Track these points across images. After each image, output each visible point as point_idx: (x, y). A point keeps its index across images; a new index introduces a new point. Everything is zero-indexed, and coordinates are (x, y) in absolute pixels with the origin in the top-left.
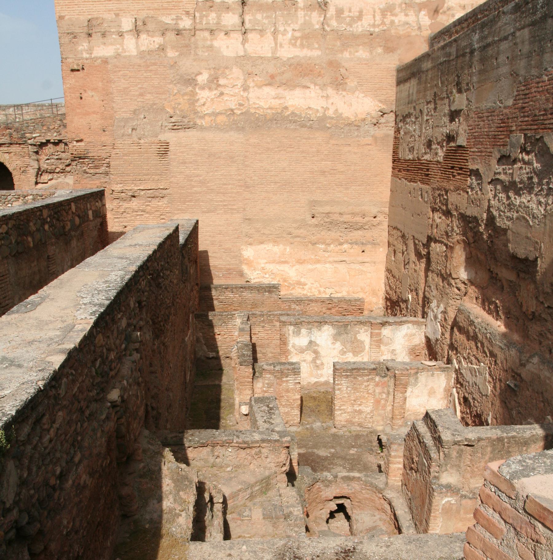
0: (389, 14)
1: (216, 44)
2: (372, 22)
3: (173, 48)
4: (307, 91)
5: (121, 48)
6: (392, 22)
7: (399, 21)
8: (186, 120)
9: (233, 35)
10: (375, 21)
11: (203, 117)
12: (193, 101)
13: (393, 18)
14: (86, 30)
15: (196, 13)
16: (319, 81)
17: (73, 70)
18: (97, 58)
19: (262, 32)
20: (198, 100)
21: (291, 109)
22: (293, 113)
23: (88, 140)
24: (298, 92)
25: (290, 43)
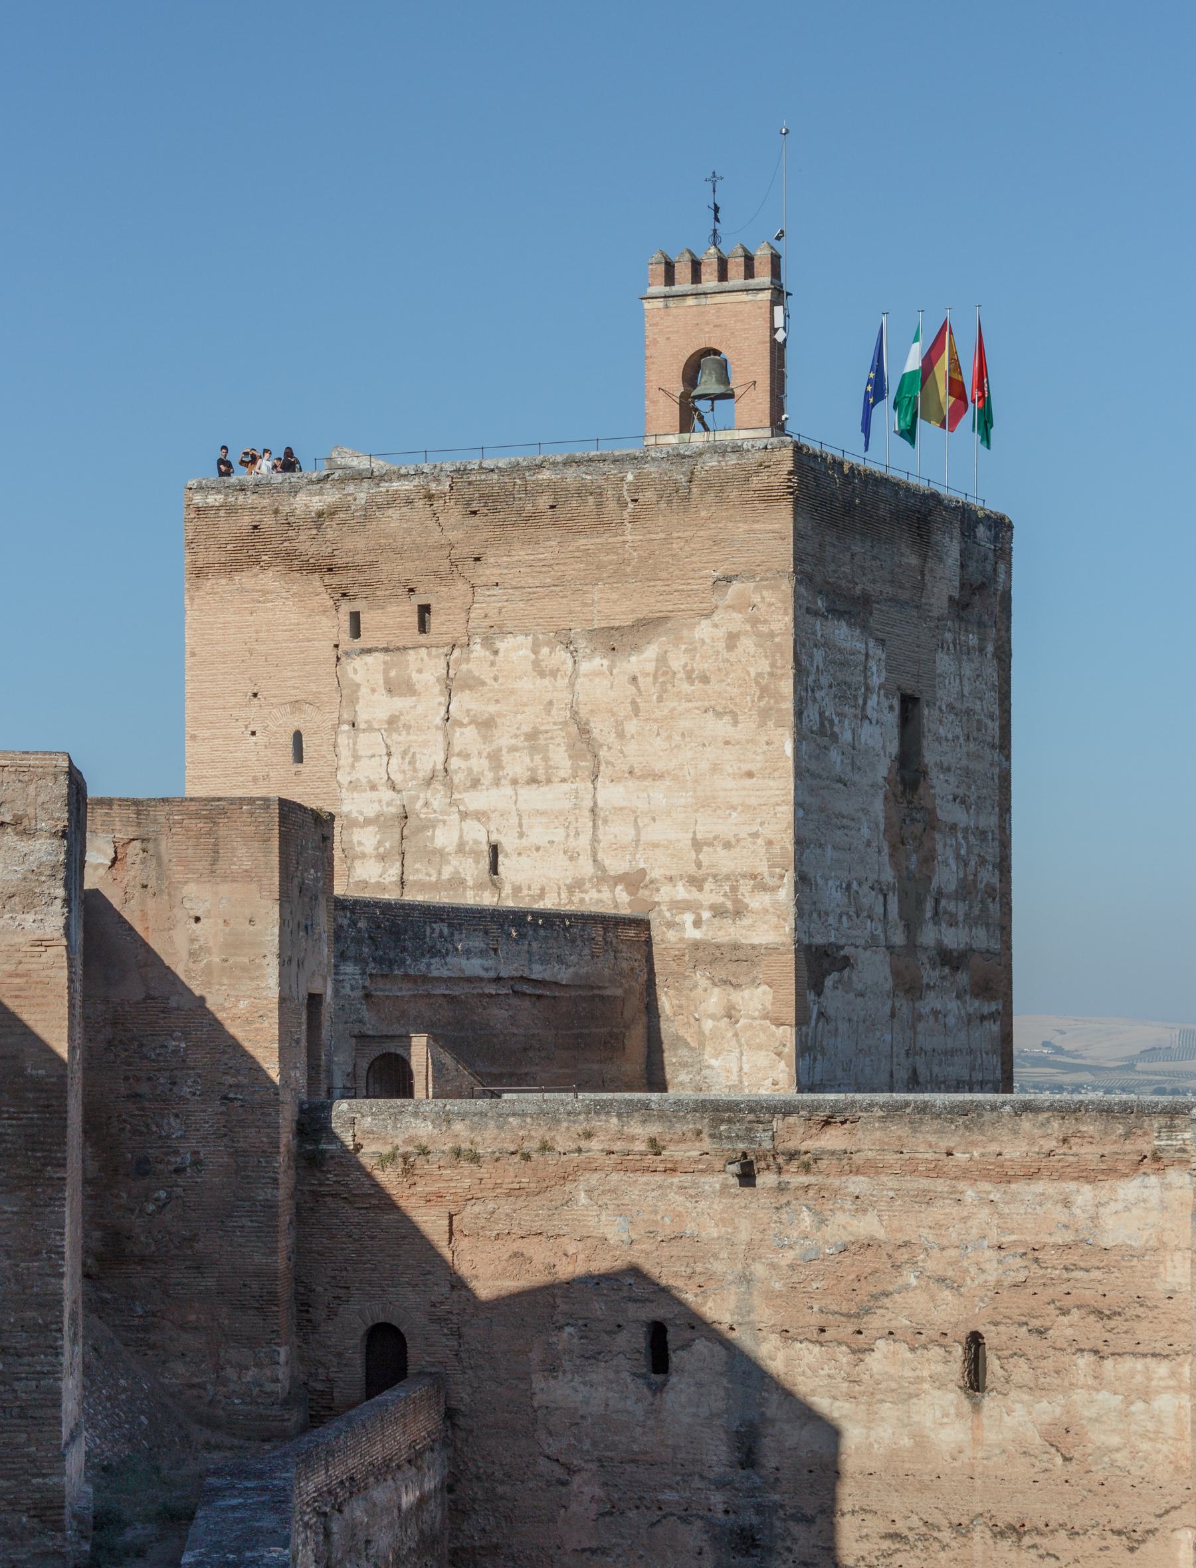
7: (591, 899)
10: (560, 899)
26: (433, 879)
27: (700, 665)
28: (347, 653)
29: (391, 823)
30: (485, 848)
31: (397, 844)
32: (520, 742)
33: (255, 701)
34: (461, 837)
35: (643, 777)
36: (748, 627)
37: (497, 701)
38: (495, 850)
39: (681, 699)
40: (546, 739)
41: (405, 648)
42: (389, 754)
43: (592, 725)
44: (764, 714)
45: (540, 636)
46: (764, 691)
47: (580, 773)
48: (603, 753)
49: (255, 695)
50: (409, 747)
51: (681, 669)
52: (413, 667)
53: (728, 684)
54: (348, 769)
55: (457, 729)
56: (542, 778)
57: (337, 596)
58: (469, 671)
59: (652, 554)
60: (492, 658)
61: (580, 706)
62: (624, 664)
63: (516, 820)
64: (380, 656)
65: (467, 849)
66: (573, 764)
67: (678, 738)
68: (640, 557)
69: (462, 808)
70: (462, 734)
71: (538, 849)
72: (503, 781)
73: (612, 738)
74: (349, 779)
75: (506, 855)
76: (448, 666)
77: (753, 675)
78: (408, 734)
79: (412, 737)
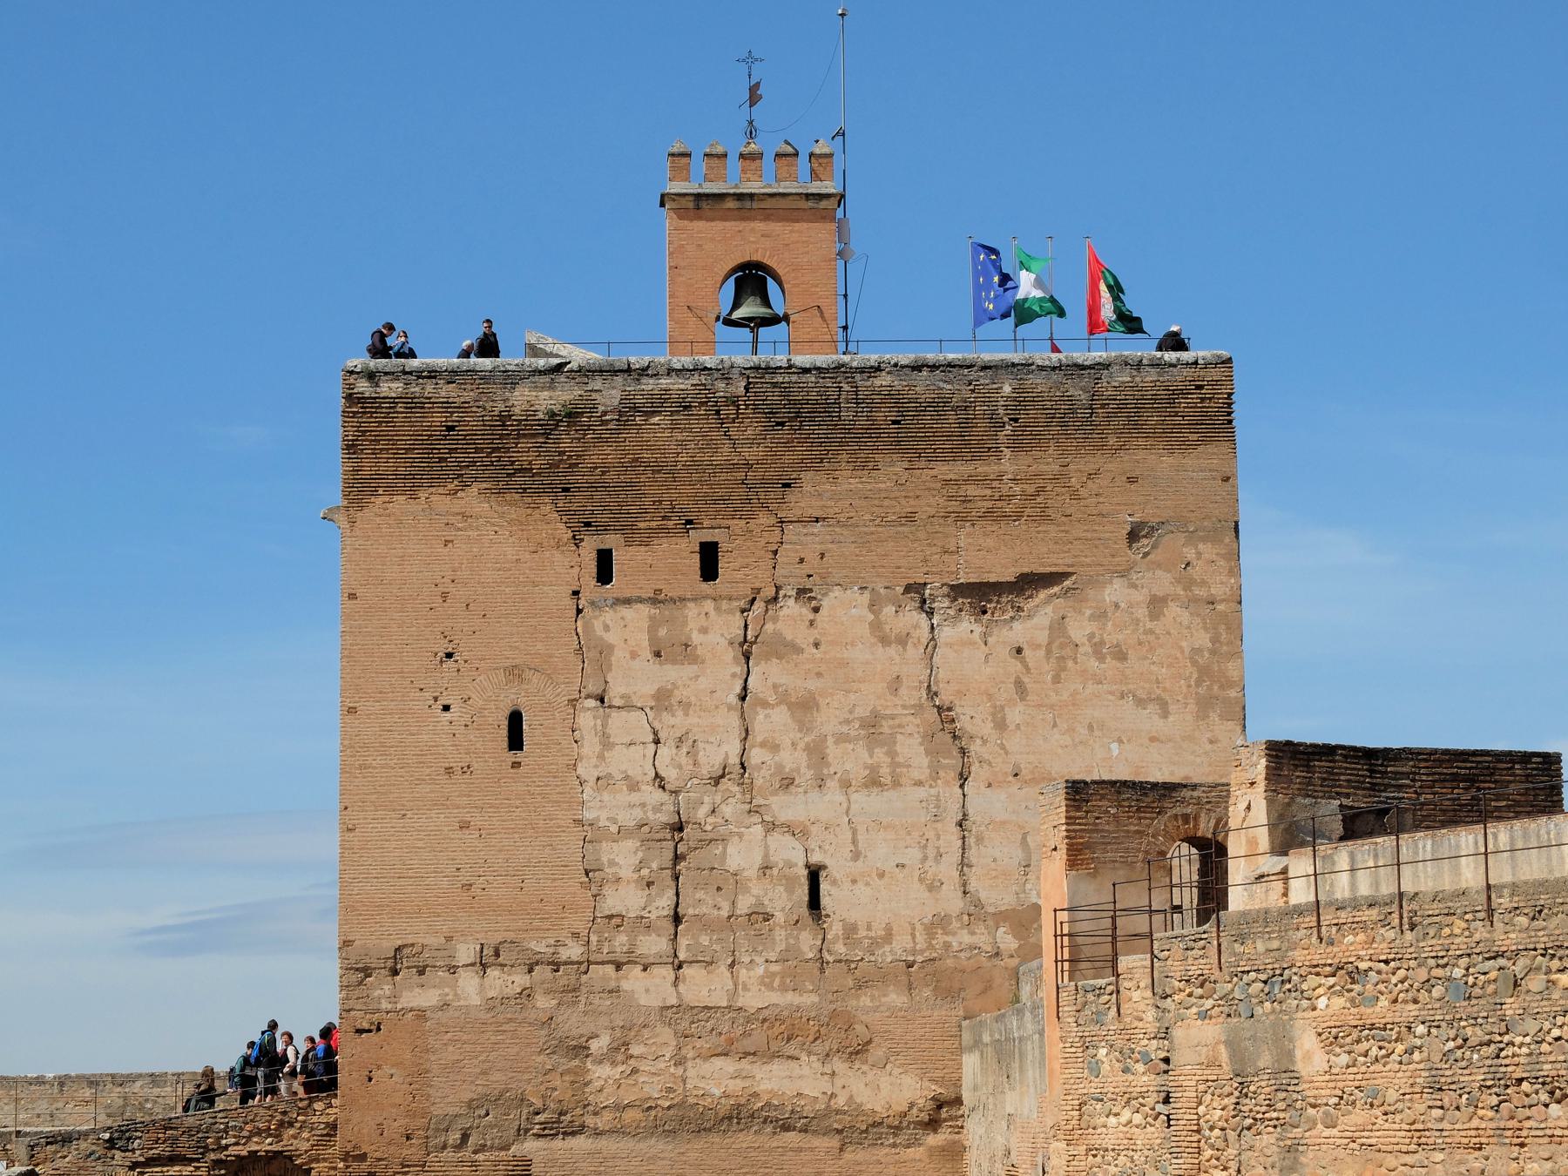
0: (940, 931)
1: (625, 985)
3: (548, 992)
5: (451, 993)
6: (947, 946)
9: (656, 970)
12: (580, 1081)
13: (949, 938)
14: (390, 963)
15: (591, 935)
18: (404, 1011)
21: (765, 1098)
22: (768, 1104)
23: (378, 1155)
24: (778, 1067)
25: (762, 983)
26: (725, 913)
27: (1112, 636)
28: (592, 603)
29: (658, 836)
30: (805, 872)
31: (669, 864)
32: (853, 730)
33: (450, 663)
34: (766, 856)
35: (1034, 781)
37: (819, 675)
38: (814, 876)
40: (891, 727)
41: (682, 600)
42: (657, 742)
43: (958, 709)
44: (1205, 705)
45: (882, 591)
46: (1204, 672)
47: (942, 774)
48: (975, 748)
49: (449, 655)
51: (1085, 640)
52: (693, 626)
53: (1154, 663)
56: (887, 780)
58: (778, 635)
59: (1040, 490)
60: (811, 616)
61: (941, 686)
63: (849, 835)
64: (645, 610)
66: (931, 761)
69: (767, 818)
70: (767, 716)
71: (881, 875)
73: (987, 729)
74: (596, 774)
75: (834, 882)
76: (746, 626)
77: (1187, 651)
79: (693, 719)
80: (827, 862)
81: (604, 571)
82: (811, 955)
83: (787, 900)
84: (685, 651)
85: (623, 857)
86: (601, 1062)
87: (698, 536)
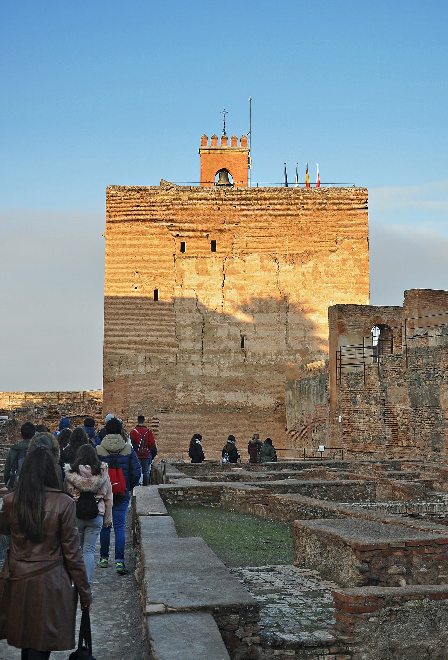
1: (187, 369)
2: (270, 359)
3: (164, 371)
4: (237, 393)
6: (281, 359)
8: (169, 408)
11: (178, 406)
13: (282, 357)
16: (243, 388)
17: (108, 381)
18: (123, 376)
19: (212, 364)
20: (177, 397)
21: (227, 402)
22: (228, 404)
24: (231, 393)
26: (217, 349)
34: (229, 332)
36: (351, 257)
37: (245, 280)
39: (323, 282)
41: (205, 257)
46: (358, 281)
47: (281, 309)
49: (137, 272)
50: (206, 296)
53: (343, 278)
54: (179, 304)
55: (228, 290)
57: (175, 235)
58: (233, 268)
60: (243, 263)
62: (300, 268)
64: (195, 260)
65: (232, 337)
67: (322, 298)
68: (306, 227)
70: (230, 292)
71: (262, 338)
72: (247, 311)
74: (180, 308)
77: (353, 275)
78: (206, 291)
80: (247, 334)
81: (183, 248)
82: (242, 361)
83: (234, 346)
84: (206, 273)
85: (187, 332)
86: (180, 392)
87: (210, 239)
